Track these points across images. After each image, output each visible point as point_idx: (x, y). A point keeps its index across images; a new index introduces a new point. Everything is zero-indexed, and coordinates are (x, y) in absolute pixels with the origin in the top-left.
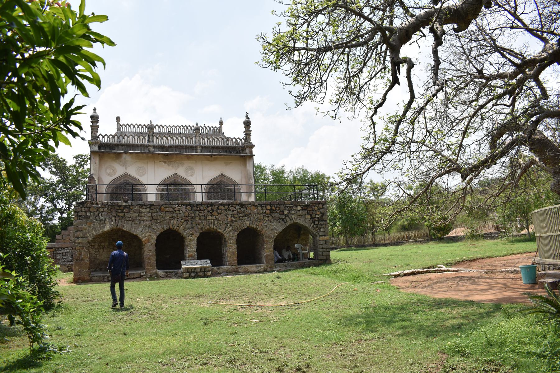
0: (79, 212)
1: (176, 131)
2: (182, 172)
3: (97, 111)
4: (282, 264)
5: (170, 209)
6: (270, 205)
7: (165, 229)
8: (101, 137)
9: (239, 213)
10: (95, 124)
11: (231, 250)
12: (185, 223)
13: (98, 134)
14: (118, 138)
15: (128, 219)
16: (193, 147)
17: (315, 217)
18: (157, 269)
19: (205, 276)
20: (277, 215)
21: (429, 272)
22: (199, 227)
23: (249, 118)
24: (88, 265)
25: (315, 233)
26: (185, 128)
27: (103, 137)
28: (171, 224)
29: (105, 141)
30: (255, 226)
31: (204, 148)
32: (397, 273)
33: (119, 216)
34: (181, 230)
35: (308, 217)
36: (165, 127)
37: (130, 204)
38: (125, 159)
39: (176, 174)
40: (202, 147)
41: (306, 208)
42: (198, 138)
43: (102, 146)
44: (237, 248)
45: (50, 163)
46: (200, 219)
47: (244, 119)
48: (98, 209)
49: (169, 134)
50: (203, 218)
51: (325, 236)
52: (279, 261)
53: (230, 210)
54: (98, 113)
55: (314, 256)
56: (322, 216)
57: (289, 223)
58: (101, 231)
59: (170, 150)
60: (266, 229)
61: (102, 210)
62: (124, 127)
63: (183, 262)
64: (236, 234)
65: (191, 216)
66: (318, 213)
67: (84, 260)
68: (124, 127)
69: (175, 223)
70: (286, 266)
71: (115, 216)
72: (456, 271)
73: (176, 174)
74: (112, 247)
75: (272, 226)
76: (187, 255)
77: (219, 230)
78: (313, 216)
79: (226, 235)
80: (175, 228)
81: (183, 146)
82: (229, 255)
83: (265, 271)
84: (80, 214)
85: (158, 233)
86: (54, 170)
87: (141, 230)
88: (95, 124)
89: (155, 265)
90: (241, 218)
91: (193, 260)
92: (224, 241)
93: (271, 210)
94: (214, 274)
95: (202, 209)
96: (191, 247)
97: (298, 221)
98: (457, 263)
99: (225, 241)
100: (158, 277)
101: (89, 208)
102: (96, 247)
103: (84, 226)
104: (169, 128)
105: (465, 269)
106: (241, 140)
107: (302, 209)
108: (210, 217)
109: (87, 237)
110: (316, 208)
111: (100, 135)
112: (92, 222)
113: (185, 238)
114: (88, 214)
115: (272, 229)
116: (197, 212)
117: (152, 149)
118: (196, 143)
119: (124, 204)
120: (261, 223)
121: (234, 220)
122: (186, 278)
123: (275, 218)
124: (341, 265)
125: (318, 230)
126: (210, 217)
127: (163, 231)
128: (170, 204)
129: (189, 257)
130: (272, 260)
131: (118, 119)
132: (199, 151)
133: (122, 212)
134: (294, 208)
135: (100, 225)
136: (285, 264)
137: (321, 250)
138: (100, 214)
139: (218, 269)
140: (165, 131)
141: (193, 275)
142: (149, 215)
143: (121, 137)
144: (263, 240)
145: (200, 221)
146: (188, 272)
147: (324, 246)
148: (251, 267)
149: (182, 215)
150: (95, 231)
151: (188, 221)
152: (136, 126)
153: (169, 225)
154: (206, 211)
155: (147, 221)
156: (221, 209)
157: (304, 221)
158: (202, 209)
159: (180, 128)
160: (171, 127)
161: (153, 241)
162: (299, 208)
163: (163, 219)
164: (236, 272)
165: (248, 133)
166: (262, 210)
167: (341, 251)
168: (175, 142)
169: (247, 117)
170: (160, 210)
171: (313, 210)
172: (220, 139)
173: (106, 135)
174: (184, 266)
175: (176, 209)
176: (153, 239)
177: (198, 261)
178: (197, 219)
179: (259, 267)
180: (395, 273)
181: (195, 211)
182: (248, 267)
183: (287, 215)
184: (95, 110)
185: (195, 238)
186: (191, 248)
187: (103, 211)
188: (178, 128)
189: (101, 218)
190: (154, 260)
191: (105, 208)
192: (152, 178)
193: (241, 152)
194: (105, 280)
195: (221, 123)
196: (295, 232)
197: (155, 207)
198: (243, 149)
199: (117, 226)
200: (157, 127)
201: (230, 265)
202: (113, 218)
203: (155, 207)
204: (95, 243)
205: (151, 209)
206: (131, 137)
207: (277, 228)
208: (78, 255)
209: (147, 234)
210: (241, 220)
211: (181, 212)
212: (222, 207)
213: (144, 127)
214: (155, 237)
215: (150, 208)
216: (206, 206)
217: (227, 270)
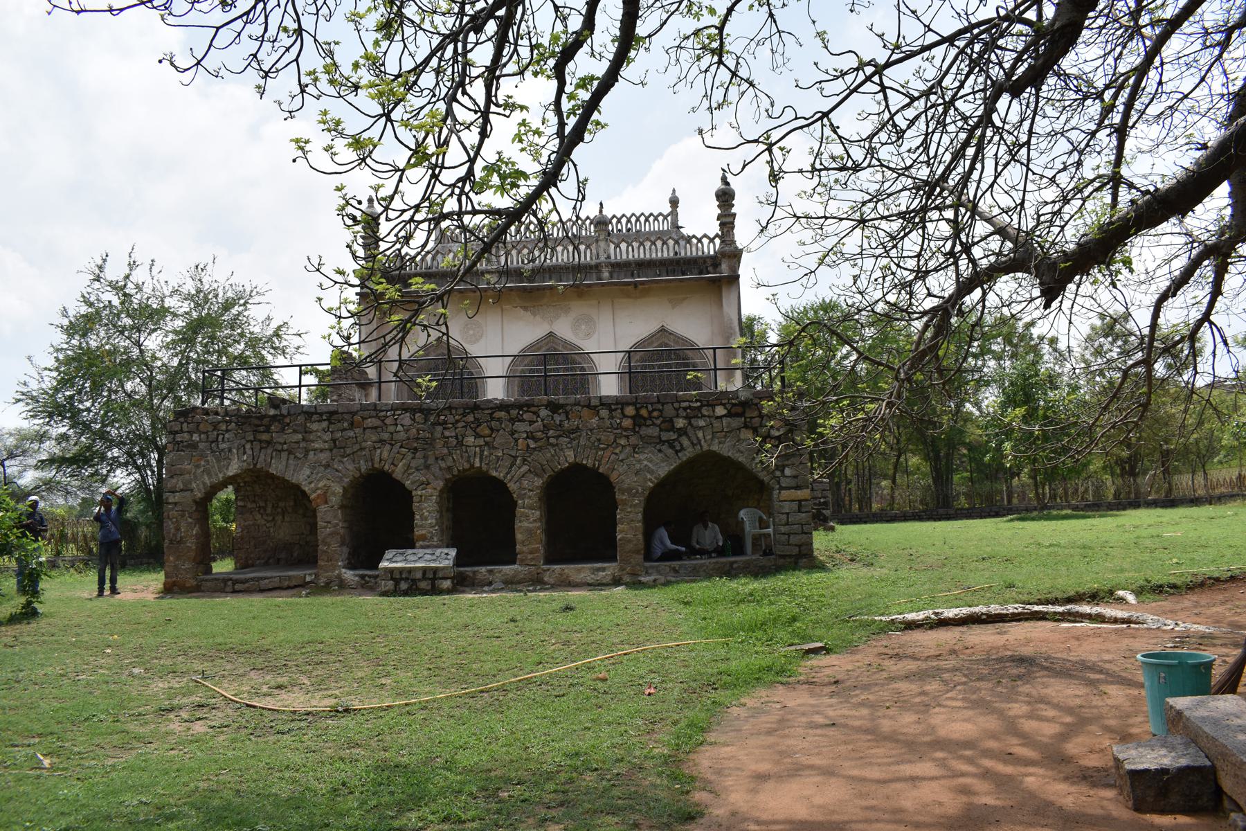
0: (177, 432)
2: (564, 328)
5: (378, 423)
6: (634, 404)
9: (546, 428)
11: (525, 524)
12: (410, 455)
15: (280, 448)
16: (591, 267)
19: (435, 591)
20: (653, 431)
21: (1041, 617)
23: (728, 184)
25: (766, 479)
28: (377, 459)
30: (588, 462)
32: (921, 616)
33: (260, 441)
34: (398, 473)
37: (285, 412)
39: (551, 335)
40: (612, 265)
42: (602, 244)
46: (446, 445)
47: (718, 184)
48: (215, 426)
50: (453, 442)
51: (797, 488)
53: (523, 421)
57: (689, 453)
58: (221, 476)
60: (622, 468)
61: (224, 428)
64: (539, 482)
69: (385, 454)
70: (676, 571)
71: (252, 442)
72: (1123, 621)
73: (551, 335)
74: (301, 511)
75: (639, 461)
77: (494, 474)
79: (512, 486)
80: (386, 467)
87: (308, 472)
90: (552, 440)
93: (637, 418)
95: (451, 419)
97: (715, 448)
98: (1202, 585)
100: (343, 586)
101: (198, 424)
102: (269, 510)
105: (1149, 617)
107: (730, 415)
112: (202, 456)
115: (638, 471)
116: (439, 428)
118: (598, 257)
119: (272, 412)
120: (608, 453)
123: (647, 440)
125: (778, 473)
126: (472, 439)
127: (357, 475)
128: (375, 409)
130: (638, 552)
132: (606, 275)
133: (268, 430)
134: (705, 411)
135: (218, 461)
138: (221, 437)
139: (490, 572)
141: (424, 585)
142: (327, 437)
145: (445, 451)
146: (392, 579)
148: (579, 571)
149: (402, 435)
151: (416, 449)
154: (460, 425)
155: (322, 451)
156: (499, 420)
162: (720, 411)
163: (357, 447)
164: (537, 582)
165: (727, 221)
166: (612, 417)
167: (1011, 520)
169: (724, 180)
170: (352, 424)
175: (388, 421)
176: (334, 494)
178: (439, 444)
179: (599, 570)
180: (911, 616)
182: (570, 570)
183: (682, 432)
186: (423, 518)
187: (227, 431)
191: (230, 422)
192: (496, 346)
194: (228, 589)
195: (674, 202)
198: (715, 261)
199: (255, 465)
202: (248, 446)
204: (266, 501)
205: (331, 423)
210: (553, 445)
211: (399, 428)
214: (338, 489)
215: (328, 419)
216: (461, 411)
217: (514, 576)
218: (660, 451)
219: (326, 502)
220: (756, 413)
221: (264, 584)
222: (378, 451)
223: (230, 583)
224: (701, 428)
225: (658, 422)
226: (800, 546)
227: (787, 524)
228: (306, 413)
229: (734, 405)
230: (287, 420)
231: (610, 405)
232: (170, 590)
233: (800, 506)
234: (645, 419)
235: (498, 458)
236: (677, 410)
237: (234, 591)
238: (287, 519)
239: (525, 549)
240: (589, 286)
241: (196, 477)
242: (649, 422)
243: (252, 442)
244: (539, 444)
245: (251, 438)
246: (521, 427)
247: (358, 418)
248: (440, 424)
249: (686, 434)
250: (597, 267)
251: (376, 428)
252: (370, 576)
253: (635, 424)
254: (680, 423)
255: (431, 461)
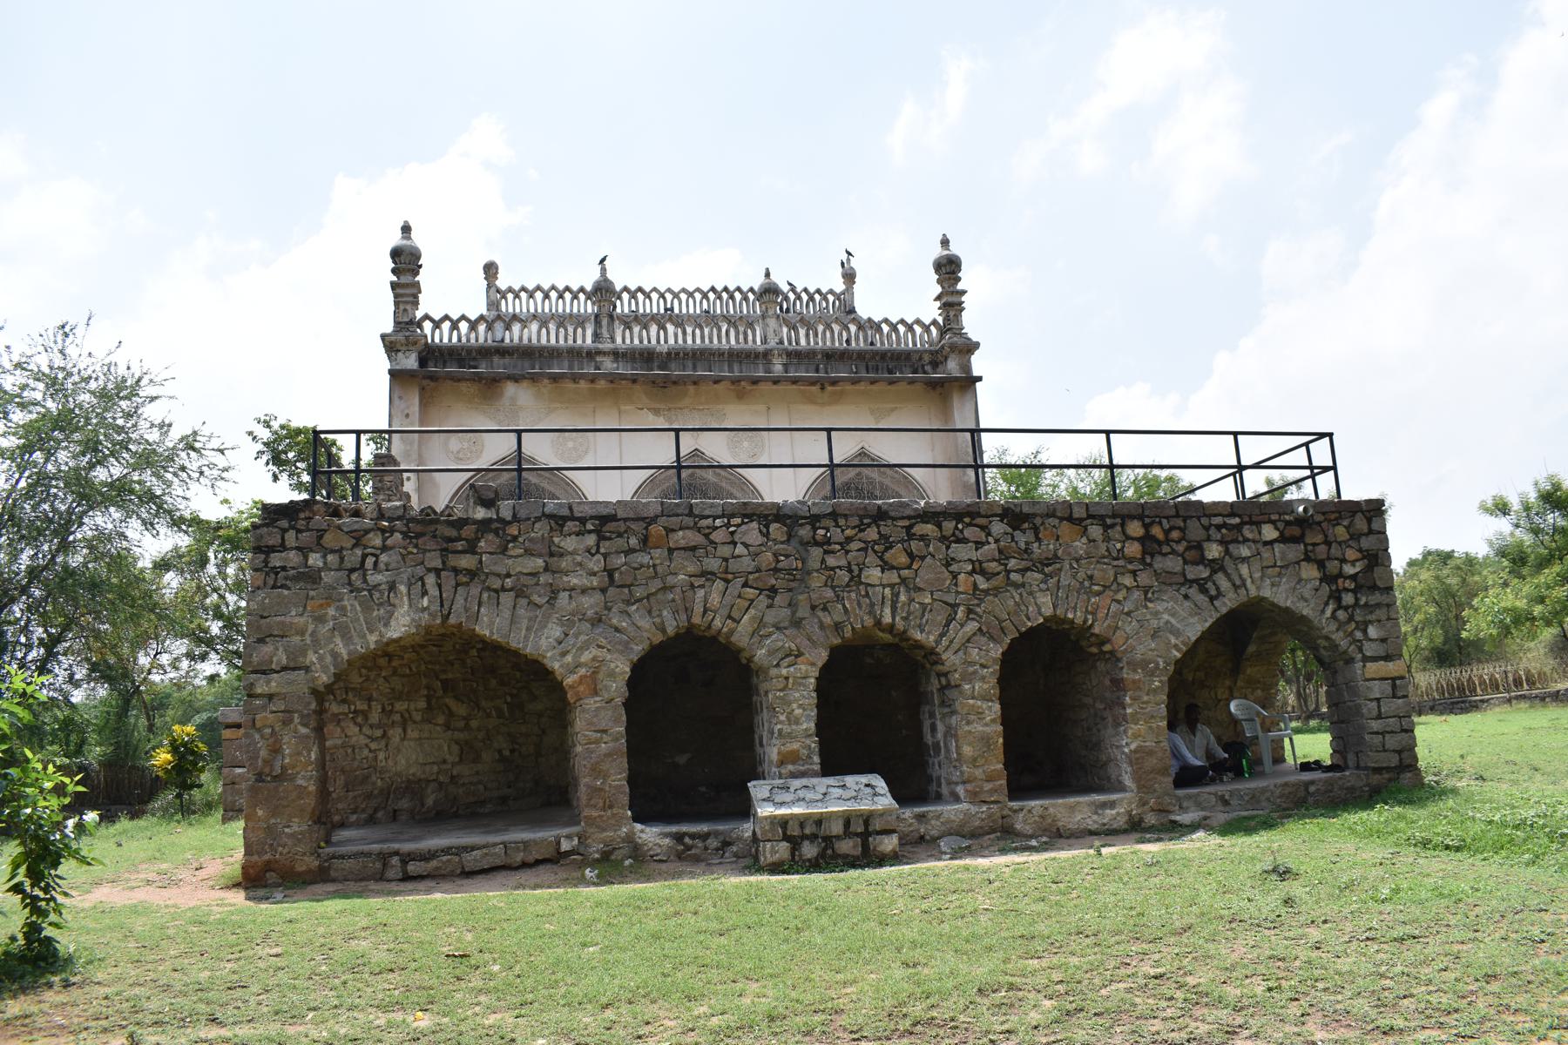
0: (271, 549)
1: (693, 308)
3: (413, 234)
4: (1207, 792)
5: (694, 538)
6: (1141, 518)
7: (671, 631)
8: (428, 326)
9: (1003, 555)
10: (405, 279)
11: (978, 728)
12: (763, 601)
13: (419, 314)
14: (489, 328)
15: (497, 584)
17: (1341, 575)
18: (636, 819)
19: (869, 858)
22: (828, 620)
24: (310, 802)
25: (1343, 644)
26: (725, 295)
27: (437, 325)
29: (444, 336)
30: (1077, 616)
31: (796, 357)
33: (456, 571)
34: (742, 634)
35: (1310, 572)
36: (654, 296)
37: (506, 514)
38: (513, 399)
40: (789, 354)
41: (1296, 531)
42: (772, 323)
43: (430, 354)
44: (1006, 720)
45: (291, 455)
46: (830, 583)
48: (358, 538)
49: (667, 318)
50: (844, 577)
51: (1387, 658)
52: (1187, 777)
53: (964, 541)
54: (418, 239)
55: (1339, 747)
56: (1369, 569)
57: (1228, 602)
59: (673, 365)
60: (1130, 627)
61: (378, 542)
62: (510, 296)
63: (758, 789)
64: (997, 651)
65: (789, 571)
66: (1351, 554)
67: (292, 778)
68: (510, 296)
69: (715, 599)
70: (1226, 803)
71: (437, 572)
74: (441, 720)
75: (1156, 614)
76: (773, 753)
77: (918, 636)
78: (1333, 567)
79: (950, 659)
80: (717, 623)
81: (720, 354)
82: (967, 750)
83: (1135, 828)
84: (276, 560)
85: (638, 649)
86: (306, 478)
87: (556, 631)
88: (405, 279)
89: (626, 800)
90: (1013, 576)
91: (803, 775)
92: (935, 684)
93: (1146, 539)
94: (917, 845)
95: (836, 534)
96: (791, 713)
97: (1267, 593)
99: (942, 689)
100: (639, 864)
101: (321, 533)
102: (375, 717)
103: (294, 617)
104: (669, 297)
106: (926, 328)
107: (1283, 539)
108: (874, 574)
109: (307, 669)
110: (1341, 532)
111: (427, 317)
112: (331, 598)
113: (762, 671)
114: (315, 559)
115: (1156, 628)
116: (816, 552)
117: (608, 365)
119: (481, 513)
120: (1104, 601)
121: (983, 585)
122: (776, 868)
123: (1166, 579)
124: (1502, 799)
125: (1359, 635)
126: (877, 572)
127: (658, 638)
128: (691, 514)
129: (782, 763)
130: (1164, 771)
131: (490, 270)
132: (778, 368)
133: (472, 549)
135: (367, 609)
136: (1220, 789)
137: (1375, 725)
138: (370, 561)
140: (655, 306)
142: (596, 564)
143: (499, 326)
144: (1118, 684)
145: (829, 594)
146: (786, 838)
147: (1389, 706)
148: (1072, 808)
149: (747, 564)
150: (347, 637)
151: (773, 591)
152: (553, 295)
153: (688, 611)
154: (855, 546)
155: (584, 591)
156: (923, 538)
157: (1292, 590)
158: (836, 534)
159: (705, 296)
160: (676, 295)
161: (616, 688)
162: (1269, 533)
163: (657, 584)
164: (1005, 836)
165: (951, 303)
166: (1107, 539)
168: (693, 339)
170: (645, 541)
171: (1328, 543)
172: (853, 328)
173: (446, 317)
174: (765, 811)
175: (718, 536)
176: (612, 675)
177: (831, 781)
178: (817, 581)
179: (1104, 805)
181: (805, 544)
183: (1216, 566)
184: (406, 229)
185: (808, 670)
187: (384, 548)
188: (698, 296)
189: (374, 578)
190: (617, 778)
191: (392, 531)
193: (932, 370)
194: (391, 874)
195: (849, 277)
196: (1241, 643)
197: (622, 527)
198: (936, 358)
200: (625, 296)
201: (975, 798)
202: (430, 580)
203: (622, 527)
204: (370, 699)
205: (601, 538)
206: (534, 326)
207: (1182, 622)
208: (263, 753)
209: (590, 656)
210: (1016, 586)
211: (740, 550)
212: (929, 529)
213: (582, 296)
214: (623, 668)
215: (598, 532)
216: (855, 521)
217: (963, 824)
218: (1186, 597)
219: (596, 693)
220: (1319, 538)
221: (471, 860)
222: (701, 593)
223: (395, 860)
224: (1244, 560)
225: (1180, 548)
226: (1399, 752)
227: (1379, 717)
228: (551, 516)
229: (1288, 523)
230: (513, 530)
231: (1102, 518)
232: (260, 878)
233: (1394, 687)
234: (1160, 543)
235: (924, 606)
236: (1207, 529)
237: (407, 878)
238: (413, 733)
239: (978, 773)
240: (755, 381)
241: (316, 643)
242: (1166, 549)
243: (437, 572)
244: (995, 582)
245: (438, 563)
246: (962, 552)
247: (656, 530)
248: (817, 544)
249: (1222, 569)
250: (767, 355)
251: (693, 549)
252: (693, 836)
253: (1144, 553)
254: (1214, 551)
255: (803, 612)
